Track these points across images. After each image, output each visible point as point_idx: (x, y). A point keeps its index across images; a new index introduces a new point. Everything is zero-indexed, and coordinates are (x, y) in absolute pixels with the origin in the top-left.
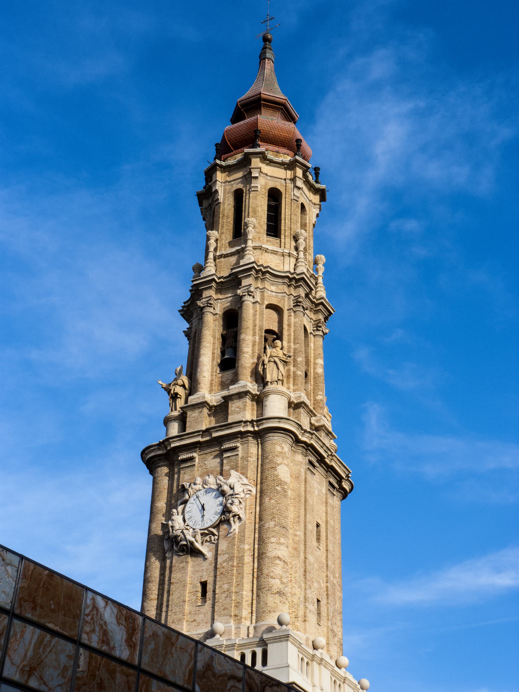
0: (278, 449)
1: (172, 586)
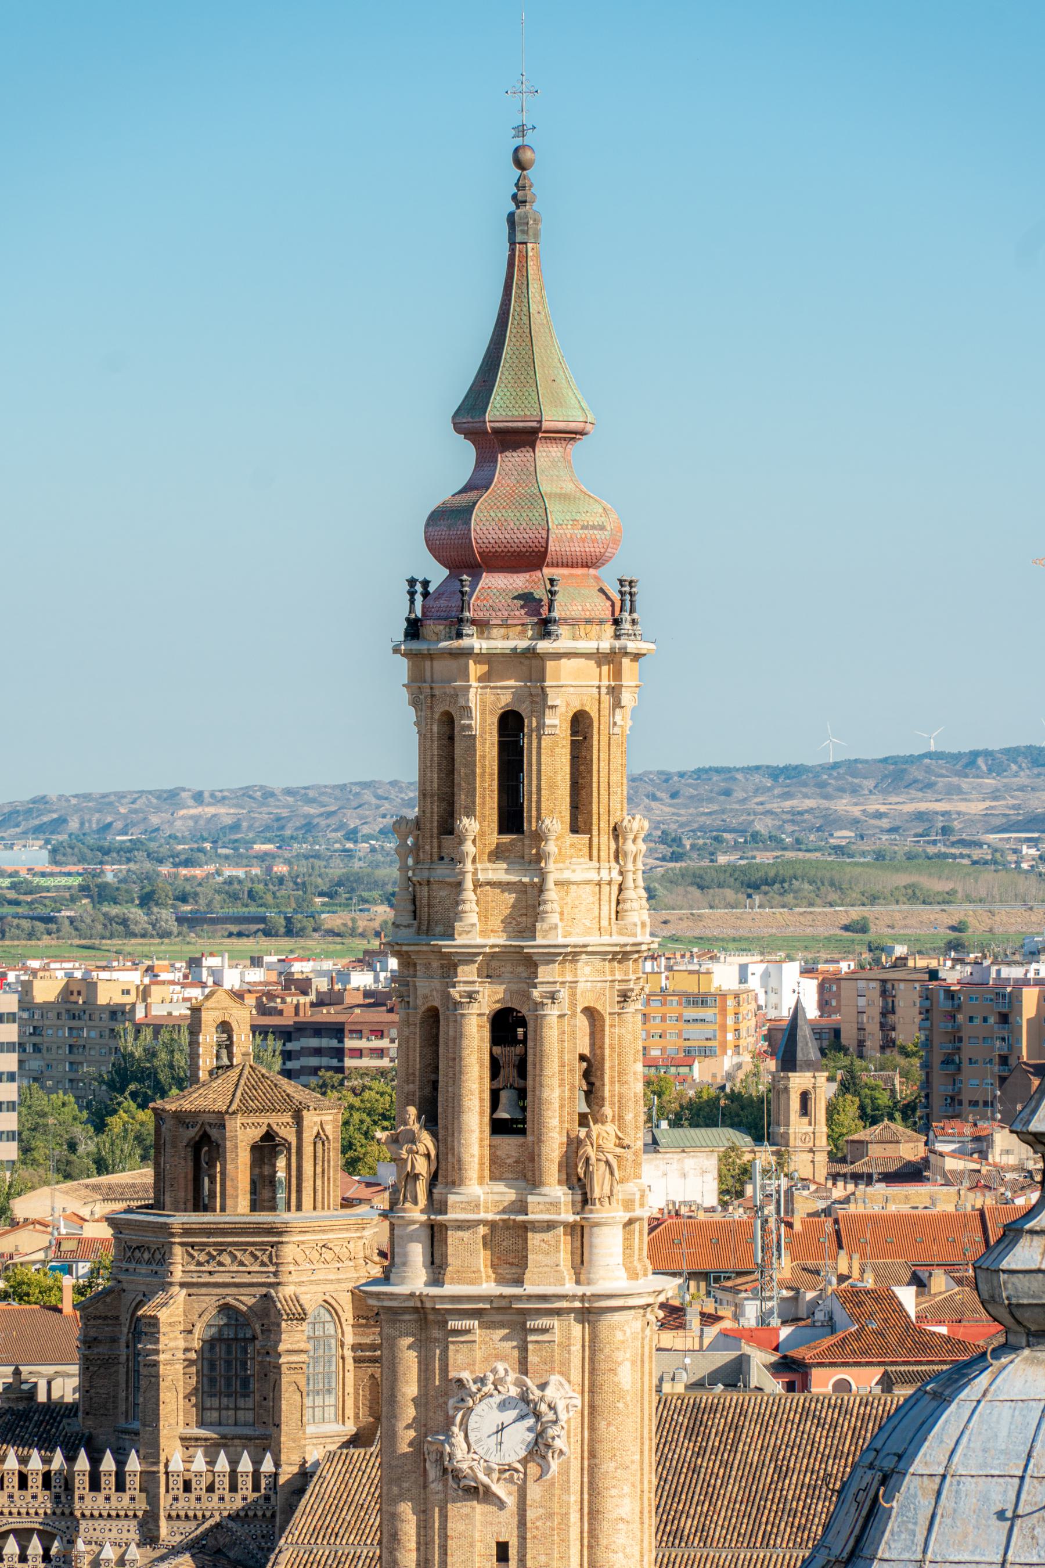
0: (619, 1336)
1: (449, 1542)
